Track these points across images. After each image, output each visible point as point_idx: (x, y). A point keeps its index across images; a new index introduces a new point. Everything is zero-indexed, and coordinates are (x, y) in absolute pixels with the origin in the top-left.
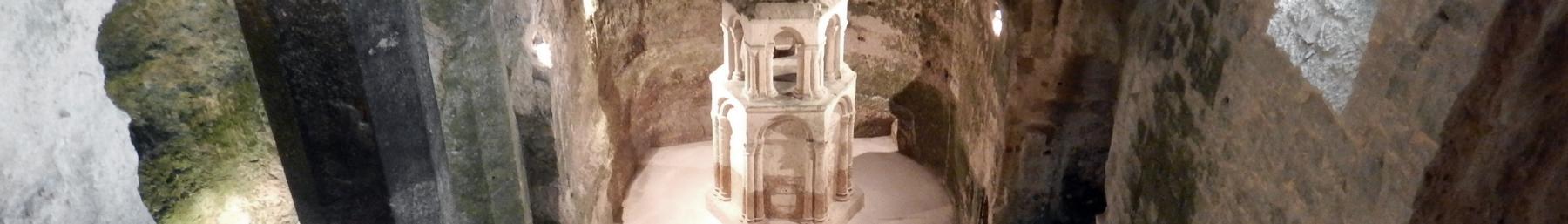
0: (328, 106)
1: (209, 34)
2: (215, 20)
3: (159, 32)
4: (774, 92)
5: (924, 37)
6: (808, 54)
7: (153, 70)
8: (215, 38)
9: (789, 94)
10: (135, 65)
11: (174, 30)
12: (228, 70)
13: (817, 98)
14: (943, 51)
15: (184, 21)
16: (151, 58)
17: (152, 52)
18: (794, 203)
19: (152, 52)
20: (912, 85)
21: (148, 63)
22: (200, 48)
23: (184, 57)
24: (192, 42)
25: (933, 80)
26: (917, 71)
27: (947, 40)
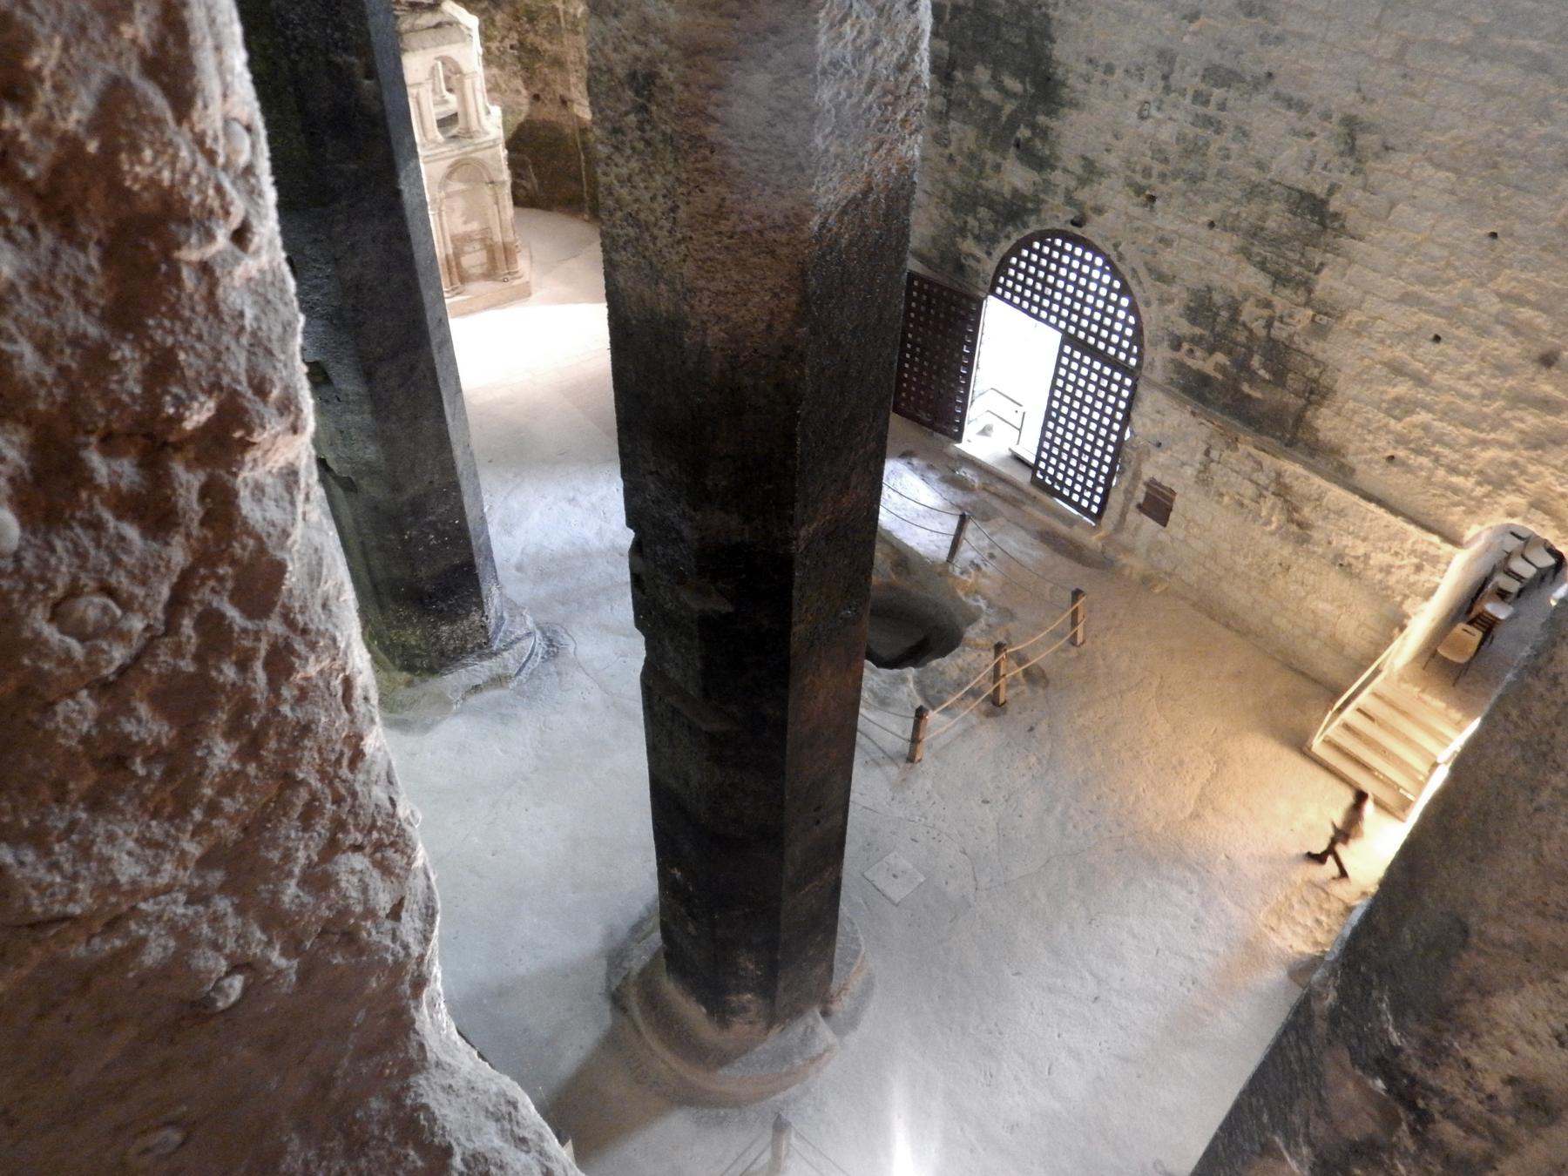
0: (330, 63)
4: (440, 138)
5: (526, 68)
6: (468, 83)
9: (454, 137)
13: (487, 133)
14: (554, 75)
18: (485, 260)
20: (521, 127)
25: (549, 112)
26: (525, 108)
27: (558, 63)
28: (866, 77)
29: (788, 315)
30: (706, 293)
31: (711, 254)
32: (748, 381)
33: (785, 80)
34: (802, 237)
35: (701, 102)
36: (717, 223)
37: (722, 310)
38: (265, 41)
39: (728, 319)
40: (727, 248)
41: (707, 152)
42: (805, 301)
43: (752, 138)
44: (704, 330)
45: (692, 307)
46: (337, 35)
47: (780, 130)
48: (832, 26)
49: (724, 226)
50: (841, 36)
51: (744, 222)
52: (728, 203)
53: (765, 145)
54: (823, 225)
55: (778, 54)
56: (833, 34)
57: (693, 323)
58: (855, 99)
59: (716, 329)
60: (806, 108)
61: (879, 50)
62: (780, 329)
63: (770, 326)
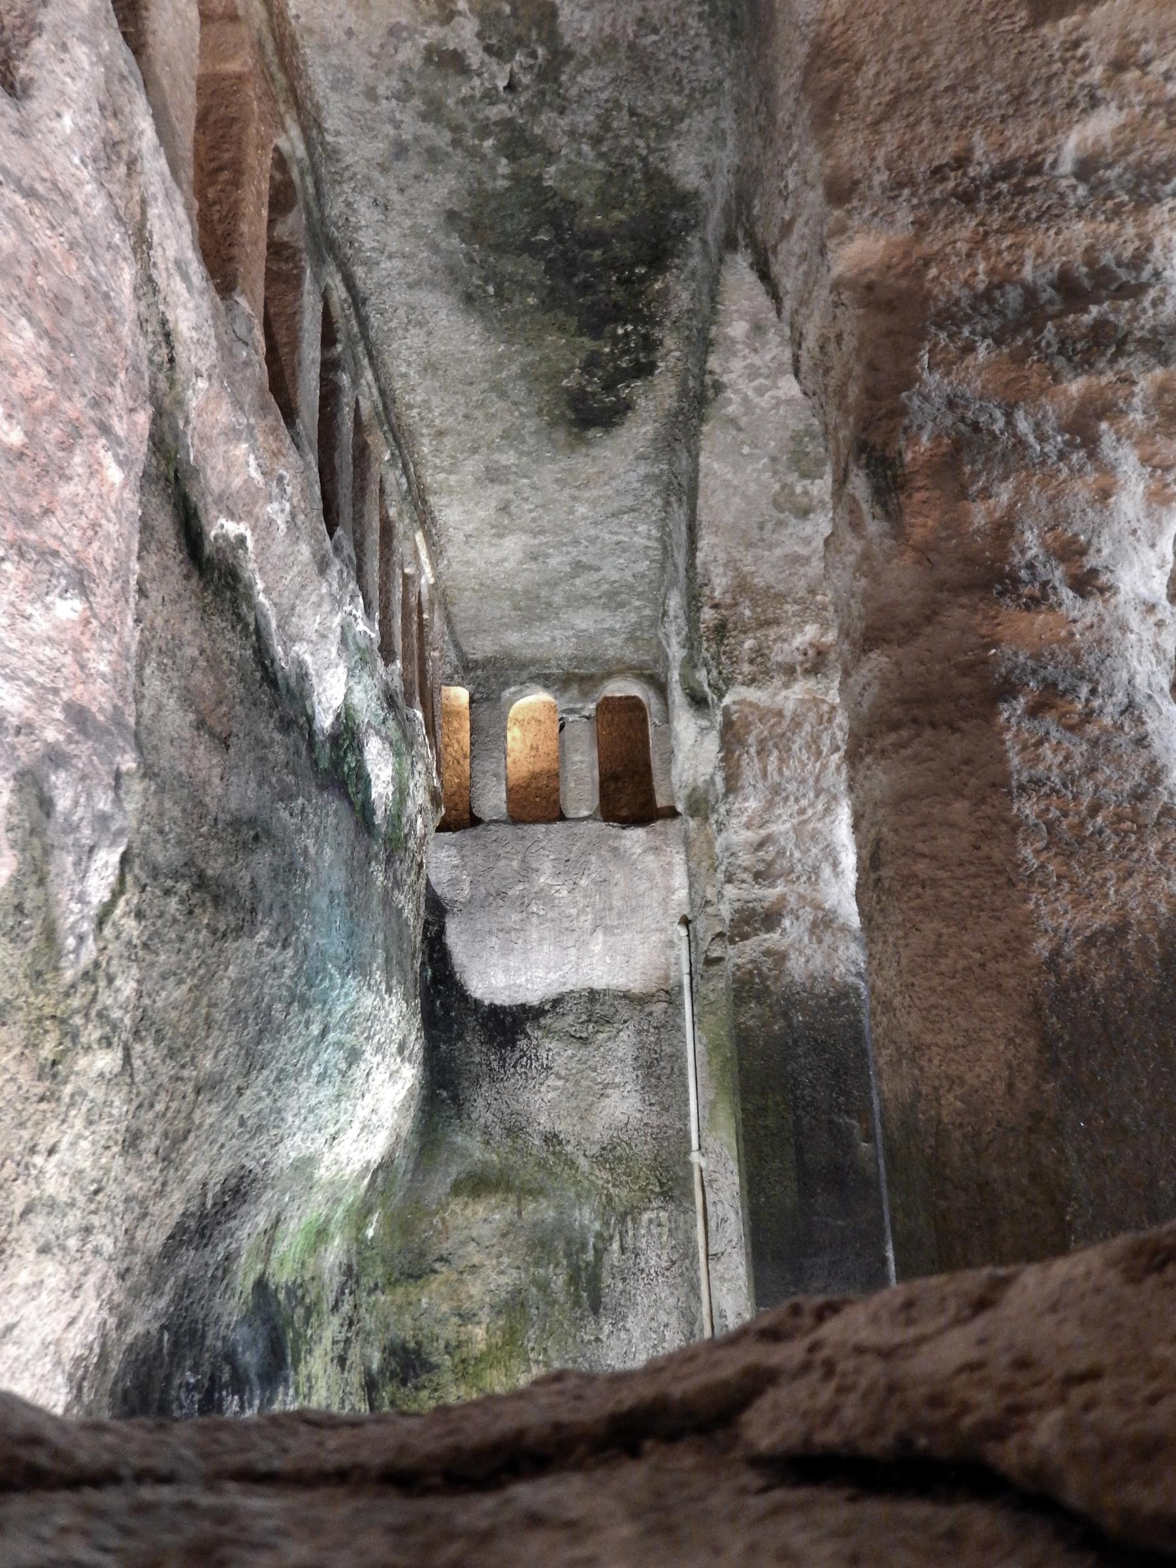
1: (495, 1250)
2: (504, 1235)
3: (448, 1245)
7: (434, 1286)
8: (499, 1256)
10: (420, 1277)
11: (463, 1244)
12: (504, 1295)
15: (474, 1233)
16: (434, 1271)
17: (437, 1266)
19: (437, 1266)
21: (432, 1277)
22: (482, 1266)
23: (465, 1275)
24: (476, 1260)
28: (1086, 801)
29: (1030, 1068)
30: (934, 1048)
31: (933, 1000)
32: (996, 1171)
33: (983, 801)
34: (1028, 962)
35: (908, 843)
36: (936, 963)
37: (953, 1070)
38: (779, 1098)
39: (962, 1081)
40: (951, 990)
41: (920, 890)
42: (1047, 1043)
43: (961, 865)
44: (938, 1099)
45: (921, 1069)
46: (842, 1099)
47: (985, 849)
48: (1024, 748)
49: (945, 964)
50: (1038, 759)
51: (965, 957)
52: (945, 939)
53: (973, 870)
54: (1057, 952)
55: (973, 781)
56: (1028, 755)
57: (925, 1090)
58: (1073, 819)
59: (950, 1097)
60: (1005, 821)
61: (1101, 777)
62: (1022, 1087)
63: (1010, 1086)
